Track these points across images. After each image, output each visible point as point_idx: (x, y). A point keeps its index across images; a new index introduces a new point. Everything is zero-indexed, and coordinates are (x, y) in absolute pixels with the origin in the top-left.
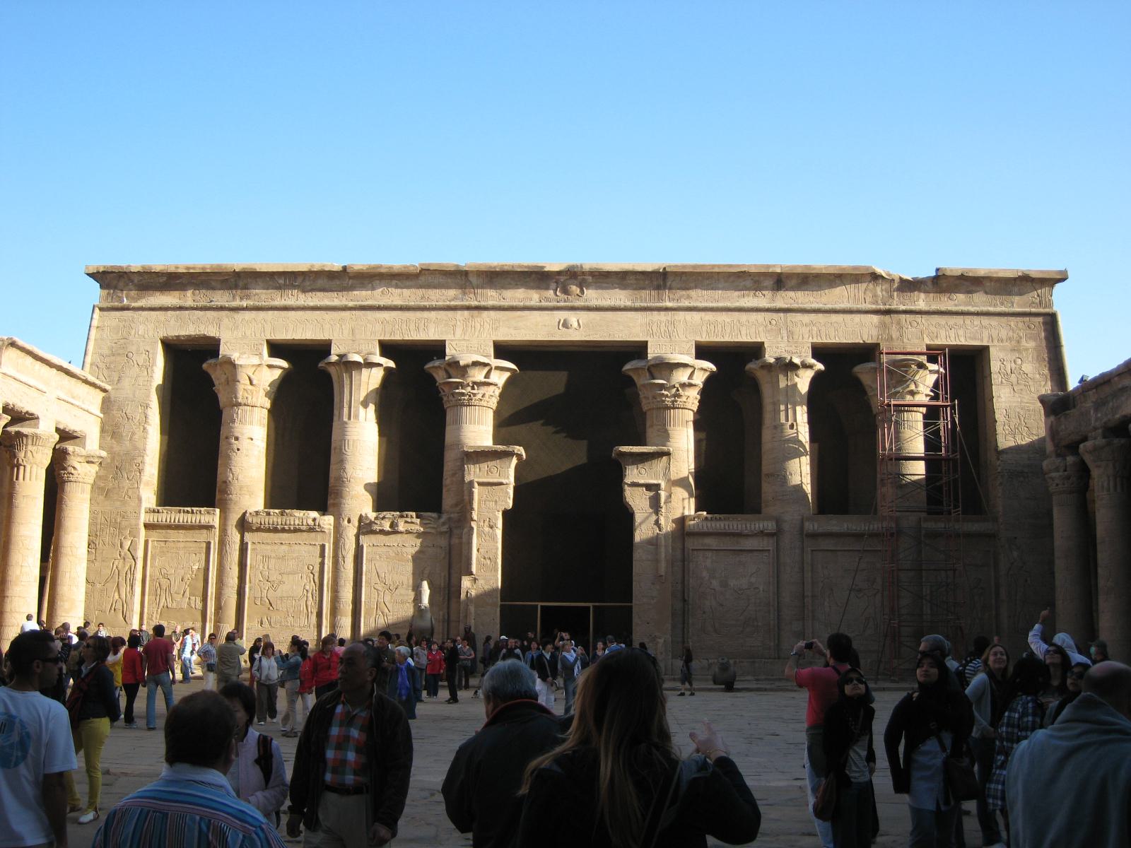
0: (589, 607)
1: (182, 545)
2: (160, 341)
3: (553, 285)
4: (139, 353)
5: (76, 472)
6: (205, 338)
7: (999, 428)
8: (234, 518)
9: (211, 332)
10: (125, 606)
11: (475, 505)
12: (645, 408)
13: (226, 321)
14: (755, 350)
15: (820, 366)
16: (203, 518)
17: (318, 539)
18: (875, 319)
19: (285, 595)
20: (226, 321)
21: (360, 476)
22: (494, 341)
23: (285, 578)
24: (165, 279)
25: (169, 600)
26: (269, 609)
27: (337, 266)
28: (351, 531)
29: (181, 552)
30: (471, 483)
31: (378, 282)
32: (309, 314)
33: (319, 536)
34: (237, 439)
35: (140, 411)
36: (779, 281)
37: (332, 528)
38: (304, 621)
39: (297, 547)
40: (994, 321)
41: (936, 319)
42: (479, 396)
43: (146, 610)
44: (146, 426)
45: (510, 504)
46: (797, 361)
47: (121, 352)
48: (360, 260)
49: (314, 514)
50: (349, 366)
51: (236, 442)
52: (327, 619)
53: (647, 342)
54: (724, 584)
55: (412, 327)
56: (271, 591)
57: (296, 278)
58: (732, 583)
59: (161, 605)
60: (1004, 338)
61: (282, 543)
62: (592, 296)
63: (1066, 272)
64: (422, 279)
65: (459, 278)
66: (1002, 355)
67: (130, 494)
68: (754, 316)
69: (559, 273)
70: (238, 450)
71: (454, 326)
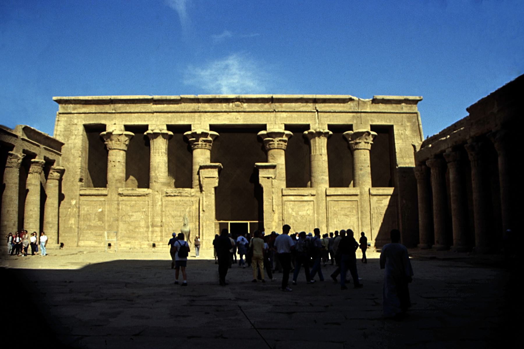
0: (247, 223)
9: (103, 122)
15: (331, 133)
33: (146, 198)
41: (373, 114)
45: (217, 185)
46: (322, 131)
54: (297, 214)
58: (300, 213)
71: (194, 119)
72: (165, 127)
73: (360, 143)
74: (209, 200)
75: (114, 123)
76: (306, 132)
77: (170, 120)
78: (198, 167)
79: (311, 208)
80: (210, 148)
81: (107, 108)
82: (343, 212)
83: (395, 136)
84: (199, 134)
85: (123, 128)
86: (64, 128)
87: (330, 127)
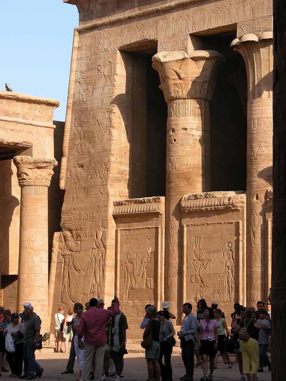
2: (118, 52)
4: (105, 66)
5: (28, 177)
8: (173, 206)
9: (150, 35)
10: (99, 288)
13: (161, 22)
19: (212, 273)
21: (265, 153)
25: (133, 282)
26: (201, 286)
33: (235, 214)
35: (107, 116)
37: (245, 205)
38: (226, 297)
39: (219, 226)
44: (111, 129)
47: (93, 66)
49: (231, 194)
51: (173, 134)
52: (243, 293)
59: (129, 286)
61: (208, 224)
86: (87, 65)
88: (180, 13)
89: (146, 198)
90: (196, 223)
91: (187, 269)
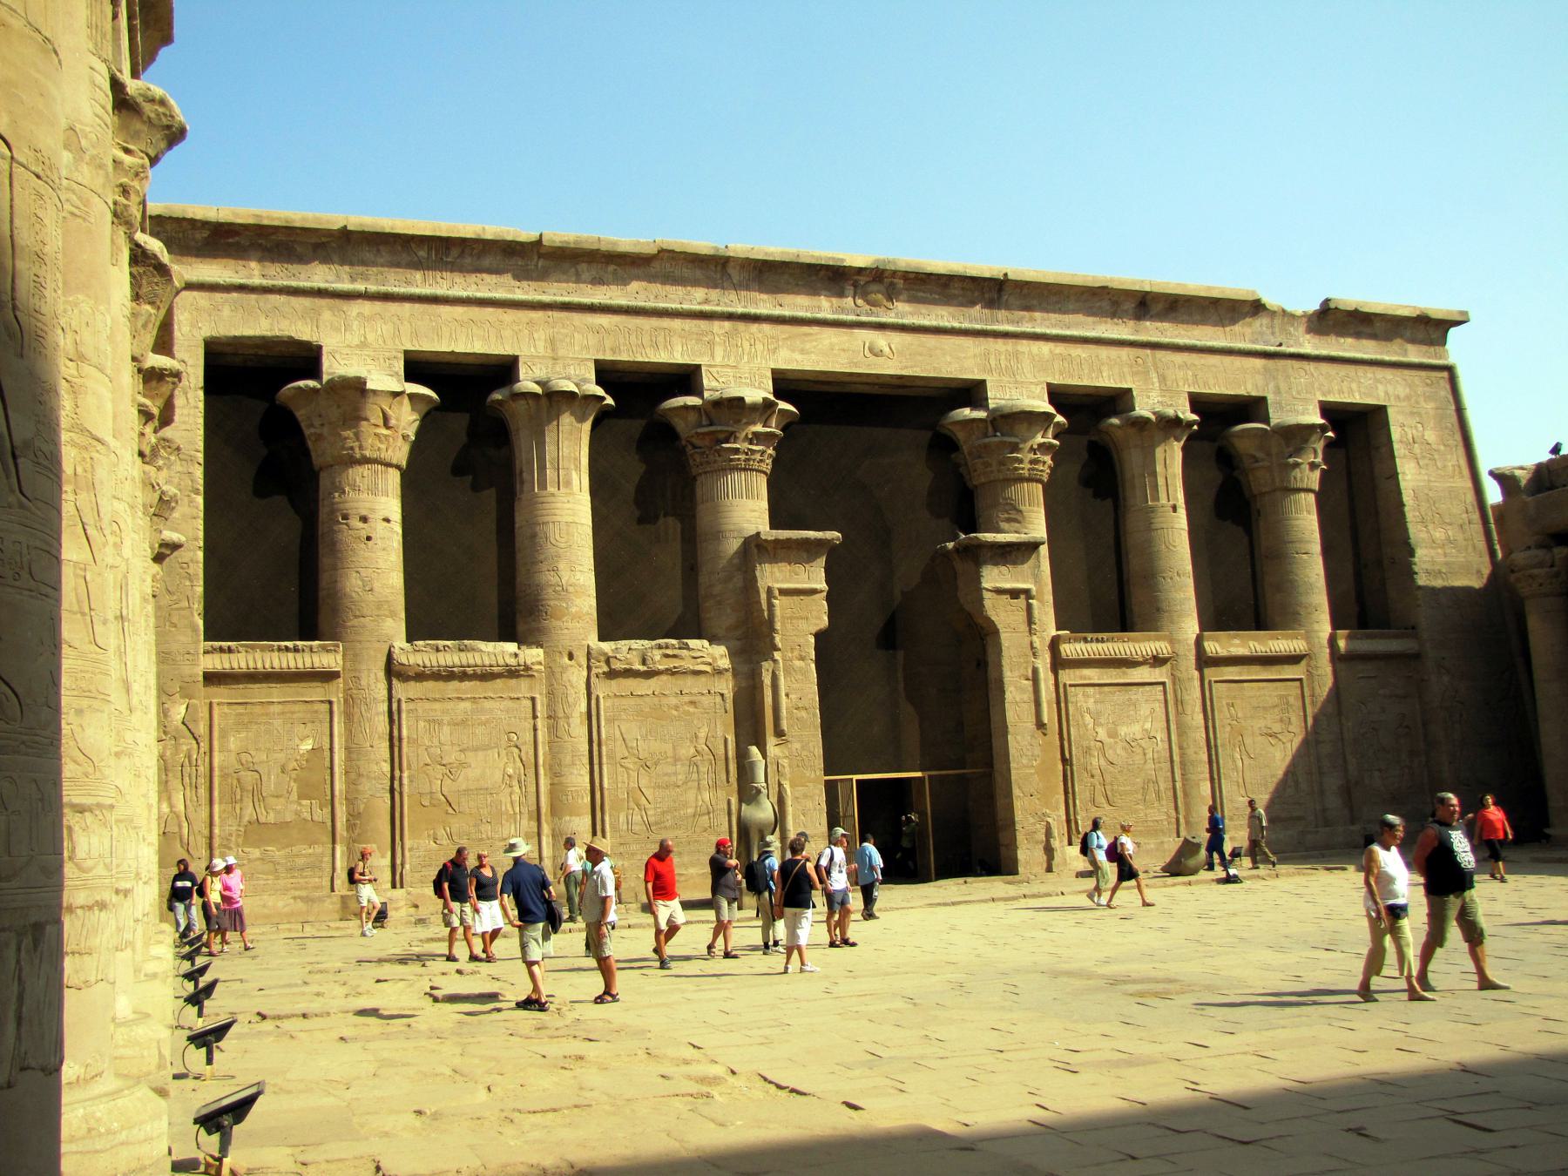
1: (276, 709)
3: (850, 290)
6: (292, 342)
7: (1410, 514)
9: (303, 331)
11: (778, 626)
12: (977, 479)
13: (327, 315)
14: (1117, 400)
16: (316, 659)
17: (522, 687)
18: (1259, 363)
20: (327, 315)
22: (774, 372)
23: (470, 757)
24: (206, 234)
27: (526, 234)
28: (576, 676)
29: (277, 723)
30: (769, 591)
31: (584, 266)
32: (475, 311)
34: (364, 519)
36: (1144, 304)
39: (487, 704)
40: (1388, 374)
41: (1325, 367)
42: (758, 457)
43: (217, 831)
45: (824, 622)
48: (561, 231)
50: (554, 400)
53: (984, 381)
54: (1113, 734)
55: (646, 340)
56: (447, 782)
57: (448, 248)
60: (1402, 395)
62: (903, 311)
63: (1465, 313)
64: (656, 266)
65: (714, 268)
66: (1401, 418)
67: (175, 620)
68: (1114, 352)
69: (860, 271)
70: (369, 538)
71: (711, 344)
72: (593, 377)
73: (1297, 465)
74: (795, 684)
75: (356, 341)
76: (1115, 421)
77: (608, 344)
78: (733, 545)
79: (1159, 708)
80: (767, 466)
81: (319, 275)
82: (1259, 724)
83: (1396, 446)
84: (754, 407)
85: (400, 366)
87: (1197, 402)
88: (378, 306)
89: (299, 643)
90: (430, 696)
91: (411, 781)
